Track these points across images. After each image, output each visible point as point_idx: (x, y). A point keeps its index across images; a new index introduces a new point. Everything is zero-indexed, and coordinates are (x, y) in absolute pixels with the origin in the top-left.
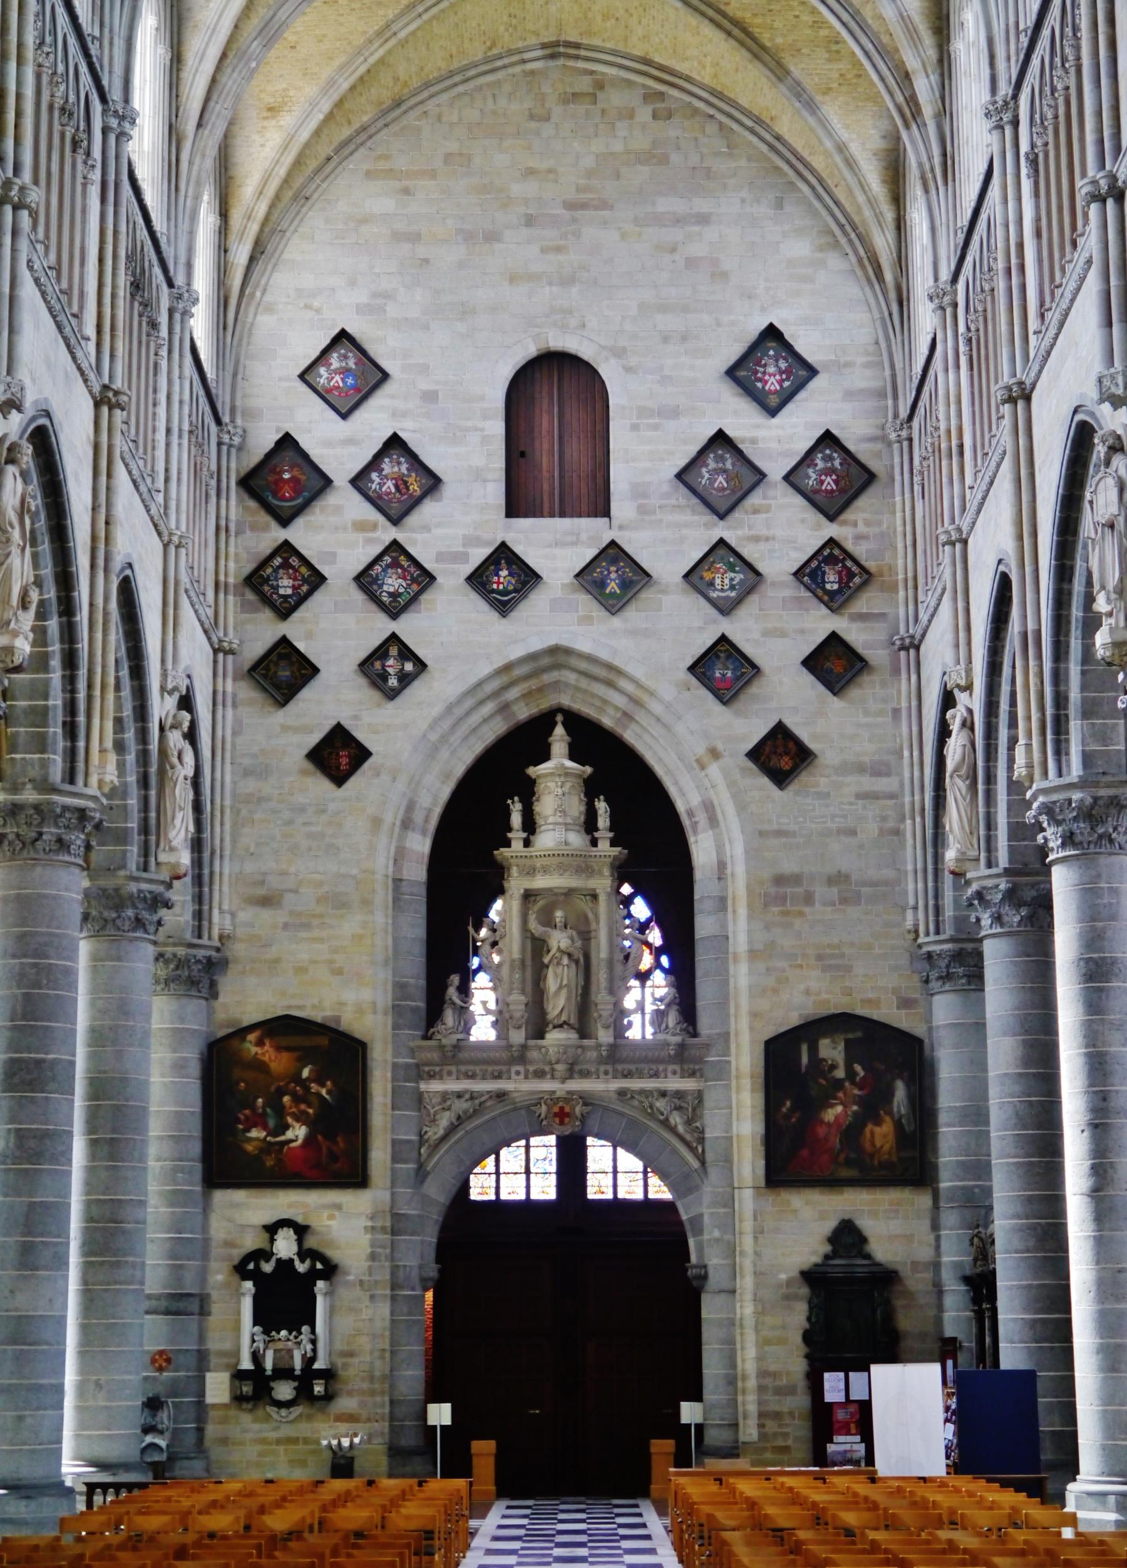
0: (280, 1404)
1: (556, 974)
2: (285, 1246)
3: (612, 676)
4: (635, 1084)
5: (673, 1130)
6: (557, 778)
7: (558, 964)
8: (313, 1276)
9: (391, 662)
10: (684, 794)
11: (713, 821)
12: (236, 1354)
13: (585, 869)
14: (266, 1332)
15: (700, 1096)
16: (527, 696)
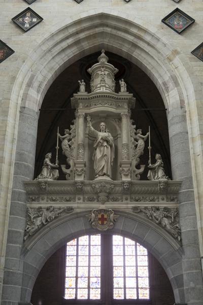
1: (101, 151)
3: (127, 27)
4: (142, 205)
5: (165, 227)
6: (103, 79)
7: (102, 146)
9: (27, 18)
10: (160, 75)
11: (176, 84)
13: (117, 101)
15: (177, 211)
16: (88, 38)
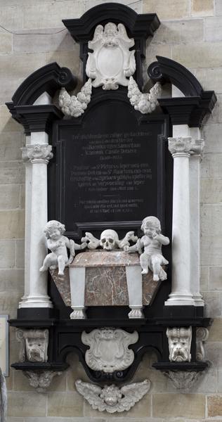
0: (102, 379)
2: (110, 61)
8: (168, 113)
12: (18, 282)
14: (74, 233)
